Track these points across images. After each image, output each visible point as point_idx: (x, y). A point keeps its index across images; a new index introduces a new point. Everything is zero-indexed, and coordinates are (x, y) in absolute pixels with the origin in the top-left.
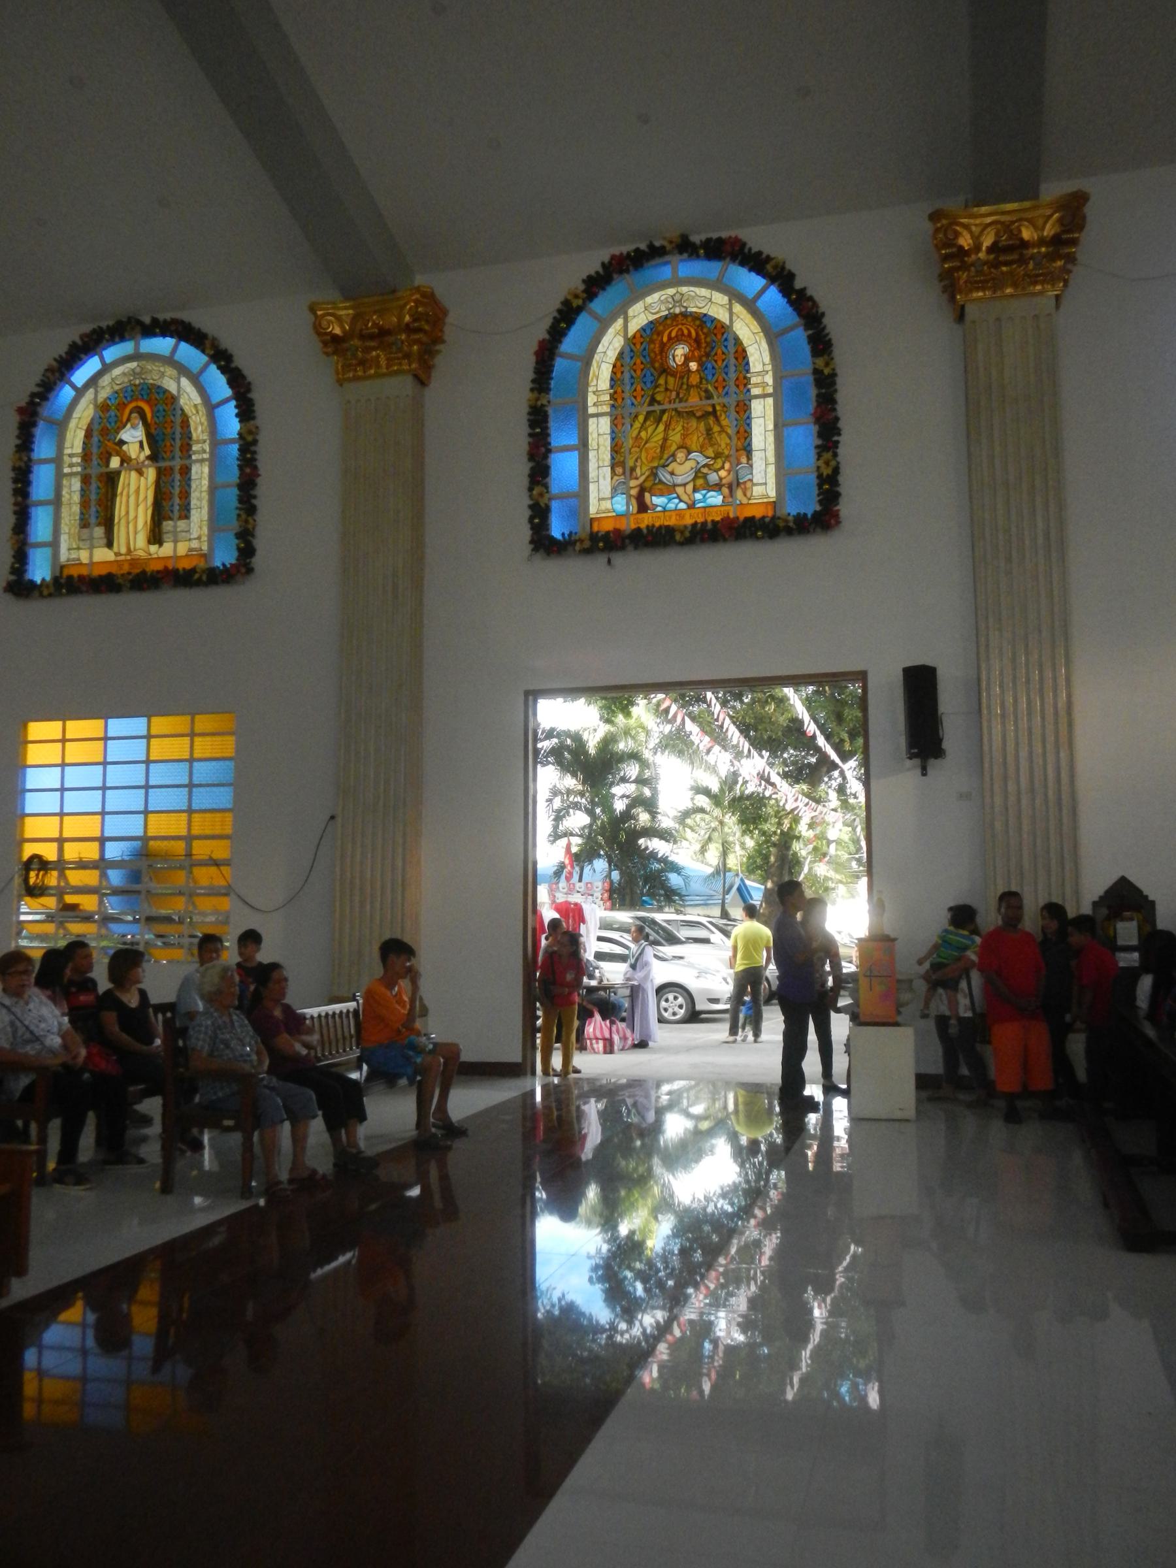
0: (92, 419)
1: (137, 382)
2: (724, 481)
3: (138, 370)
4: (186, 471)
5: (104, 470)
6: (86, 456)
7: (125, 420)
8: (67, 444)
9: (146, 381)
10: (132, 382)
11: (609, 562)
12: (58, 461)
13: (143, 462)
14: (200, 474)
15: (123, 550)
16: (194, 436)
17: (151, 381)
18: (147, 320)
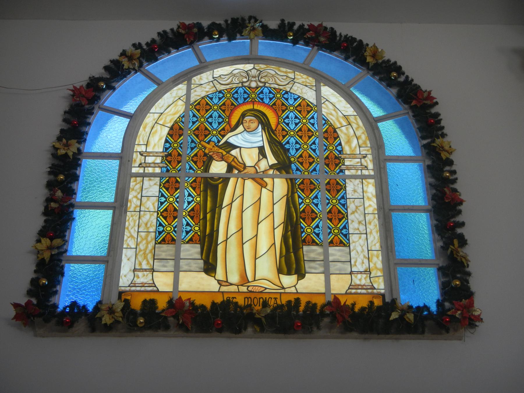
1: (253, 85)
3: (254, 72)
7: (234, 122)
9: (267, 85)
15: (234, 278)
16: (347, 149)
17: (277, 87)
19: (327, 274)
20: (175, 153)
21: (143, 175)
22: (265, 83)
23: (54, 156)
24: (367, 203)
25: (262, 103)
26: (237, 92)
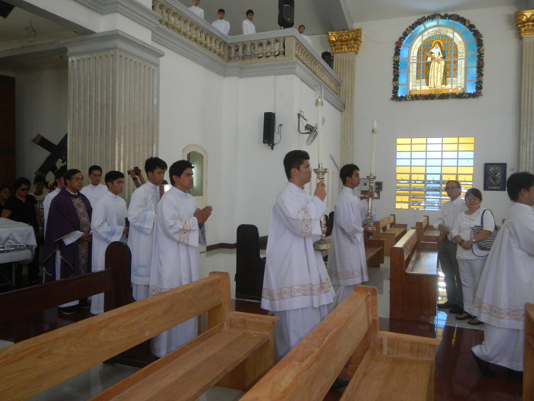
0: (421, 45)
1: (438, 34)
3: (438, 30)
4: (456, 62)
5: (425, 61)
6: (418, 57)
7: (433, 46)
8: (412, 53)
13: (439, 59)
14: (461, 64)
15: (432, 86)
16: (459, 51)
17: (443, 34)
18: (443, 14)
21: (413, 63)
23: (394, 60)
24: (462, 66)
25: (440, 40)
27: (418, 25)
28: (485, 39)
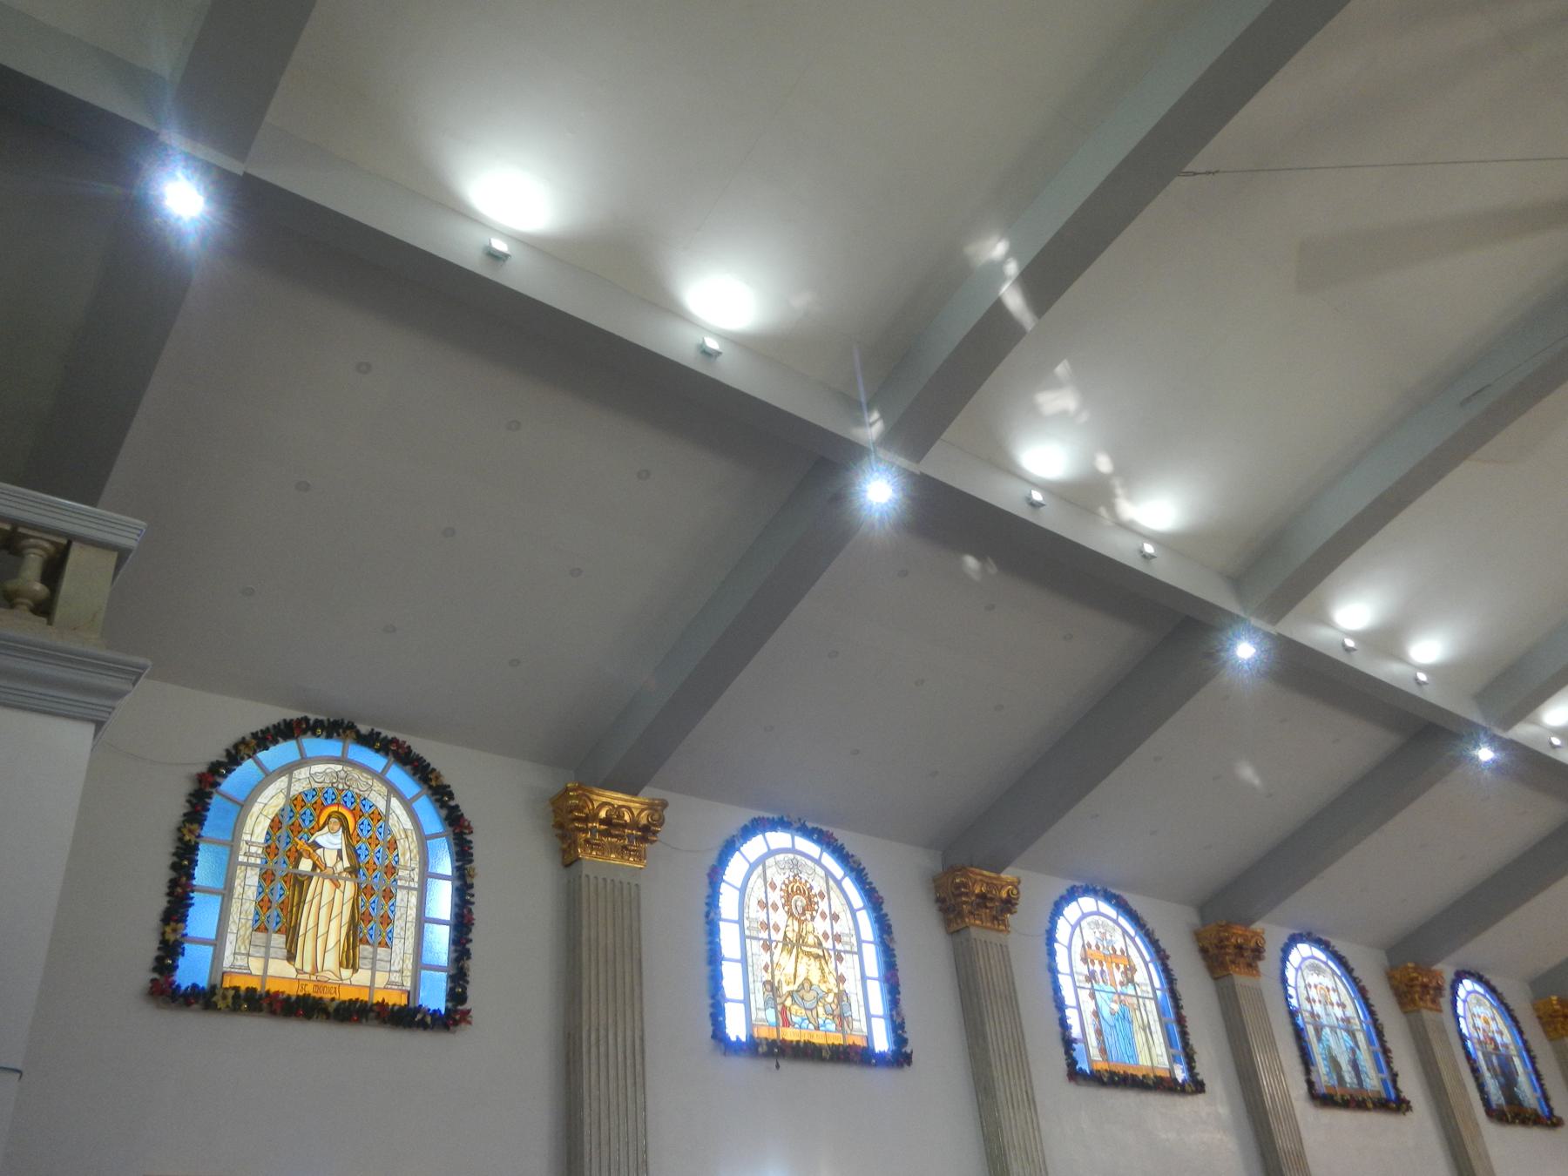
1: (341, 787)
2: (835, 1013)
3: (342, 774)
4: (389, 895)
6: (270, 849)
8: (248, 828)
10: (335, 785)
11: (778, 1066)
12: (232, 845)
15: (308, 968)
16: (402, 862)
17: (358, 791)
19: (373, 970)
20: (273, 846)
22: (349, 787)
23: (181, 839)
25: (346, 807)
26: (327, 792)
27: (279, 739)
28: (478, 841)
